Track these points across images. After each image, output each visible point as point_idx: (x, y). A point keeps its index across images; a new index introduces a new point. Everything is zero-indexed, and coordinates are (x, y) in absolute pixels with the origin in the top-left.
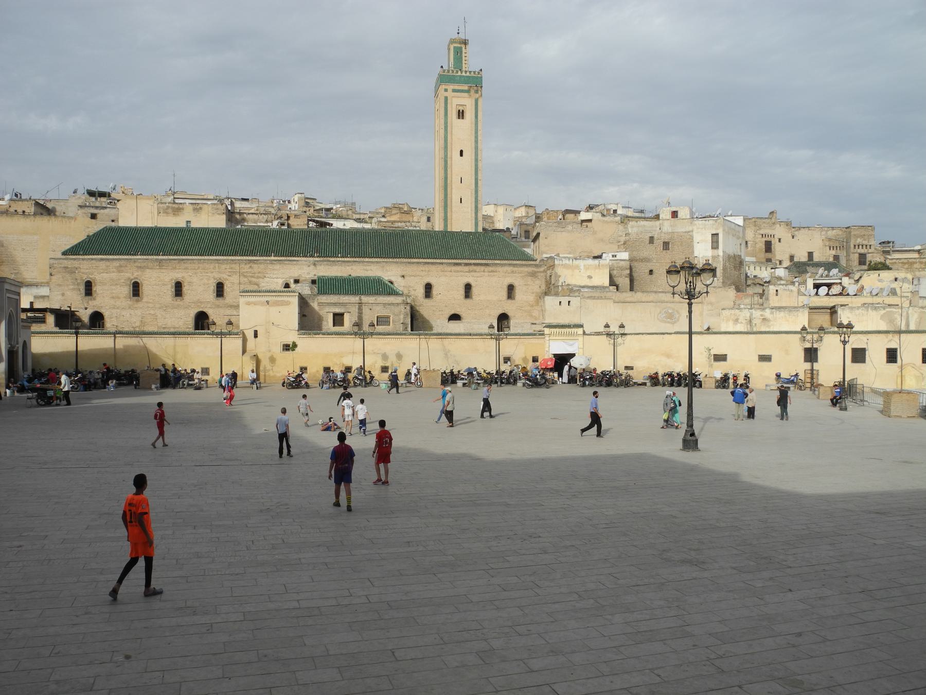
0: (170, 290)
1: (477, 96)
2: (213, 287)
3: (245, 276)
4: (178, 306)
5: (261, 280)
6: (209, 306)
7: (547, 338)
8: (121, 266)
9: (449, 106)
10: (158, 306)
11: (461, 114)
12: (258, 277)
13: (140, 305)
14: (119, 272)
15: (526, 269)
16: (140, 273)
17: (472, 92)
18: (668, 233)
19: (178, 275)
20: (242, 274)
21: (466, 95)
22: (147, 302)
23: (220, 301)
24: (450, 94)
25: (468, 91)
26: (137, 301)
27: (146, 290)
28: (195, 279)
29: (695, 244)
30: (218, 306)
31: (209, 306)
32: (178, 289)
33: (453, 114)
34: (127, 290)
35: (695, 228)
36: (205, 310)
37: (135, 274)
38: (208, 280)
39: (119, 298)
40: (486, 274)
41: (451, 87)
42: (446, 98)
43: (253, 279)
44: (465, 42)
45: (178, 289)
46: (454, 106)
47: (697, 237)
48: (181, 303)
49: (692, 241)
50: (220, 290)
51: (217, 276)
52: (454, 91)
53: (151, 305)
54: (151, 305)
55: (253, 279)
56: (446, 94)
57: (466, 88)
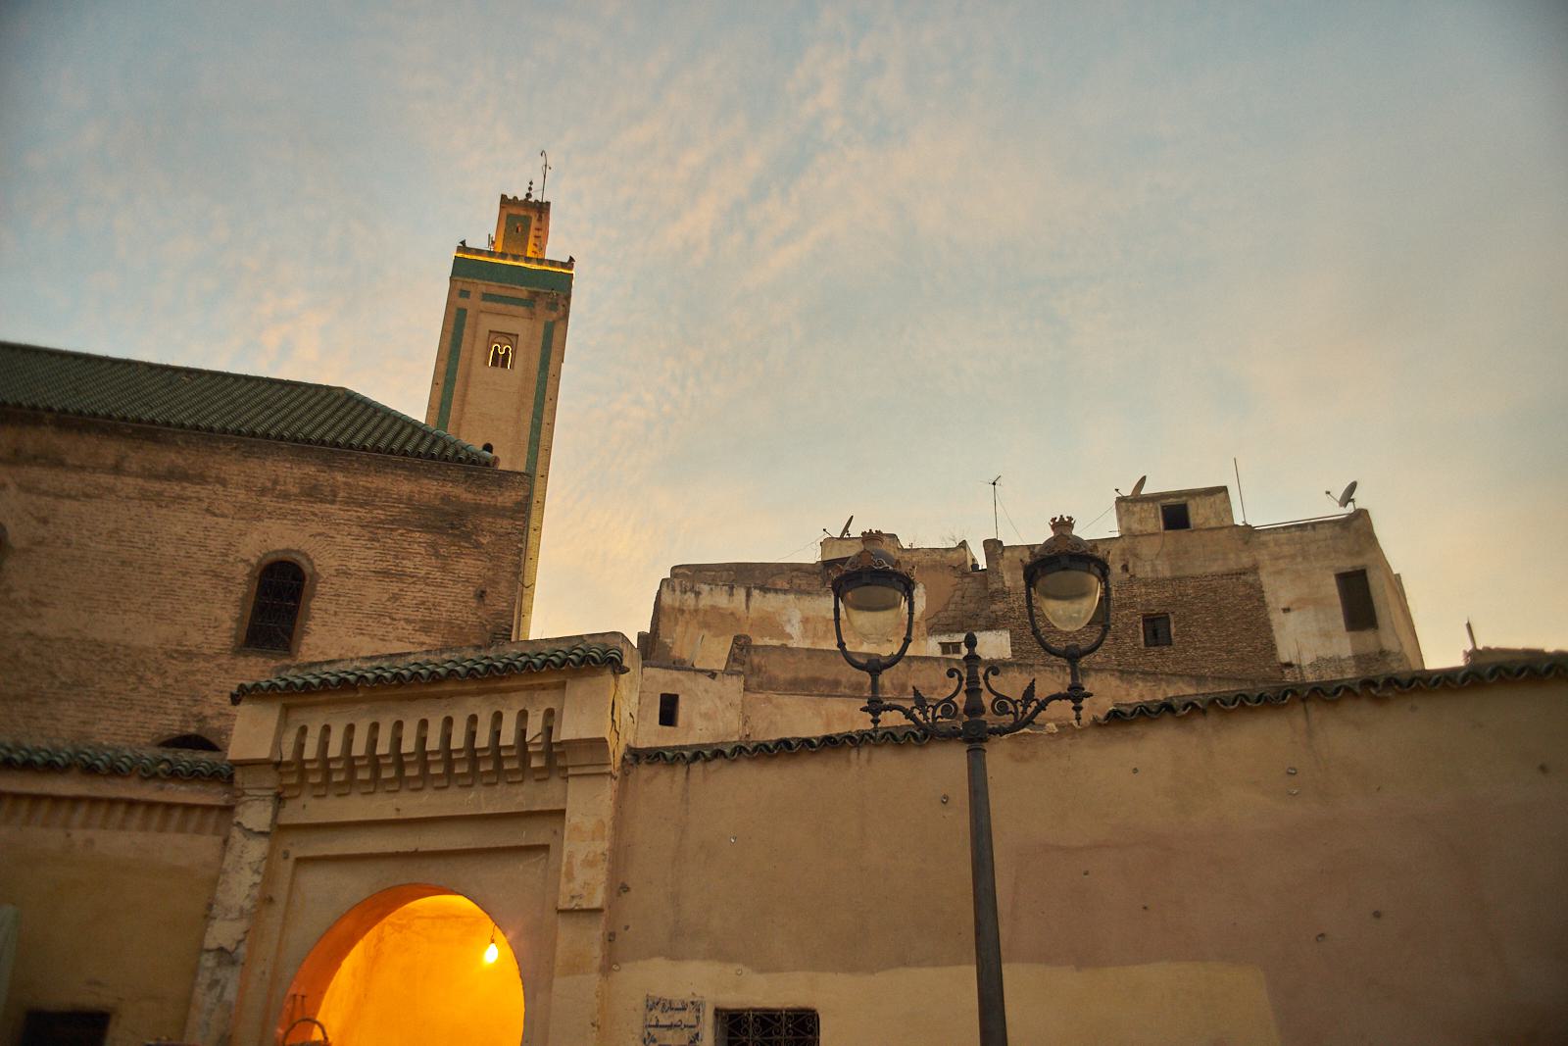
1: (554, 315)
7: (256, 815)
9: (467, 332)
15: (405, 487)
18: (1159, 583)
21: (521, 310)
25: (529, 303)
29: (1276, 618)
35: (1263, 556)
40: (129, 484)
44: (543, 208)
46: (483, 332)
47: (1278, 591)
49: (1262, 604)
52: (486, 297)
56: (462, 302)
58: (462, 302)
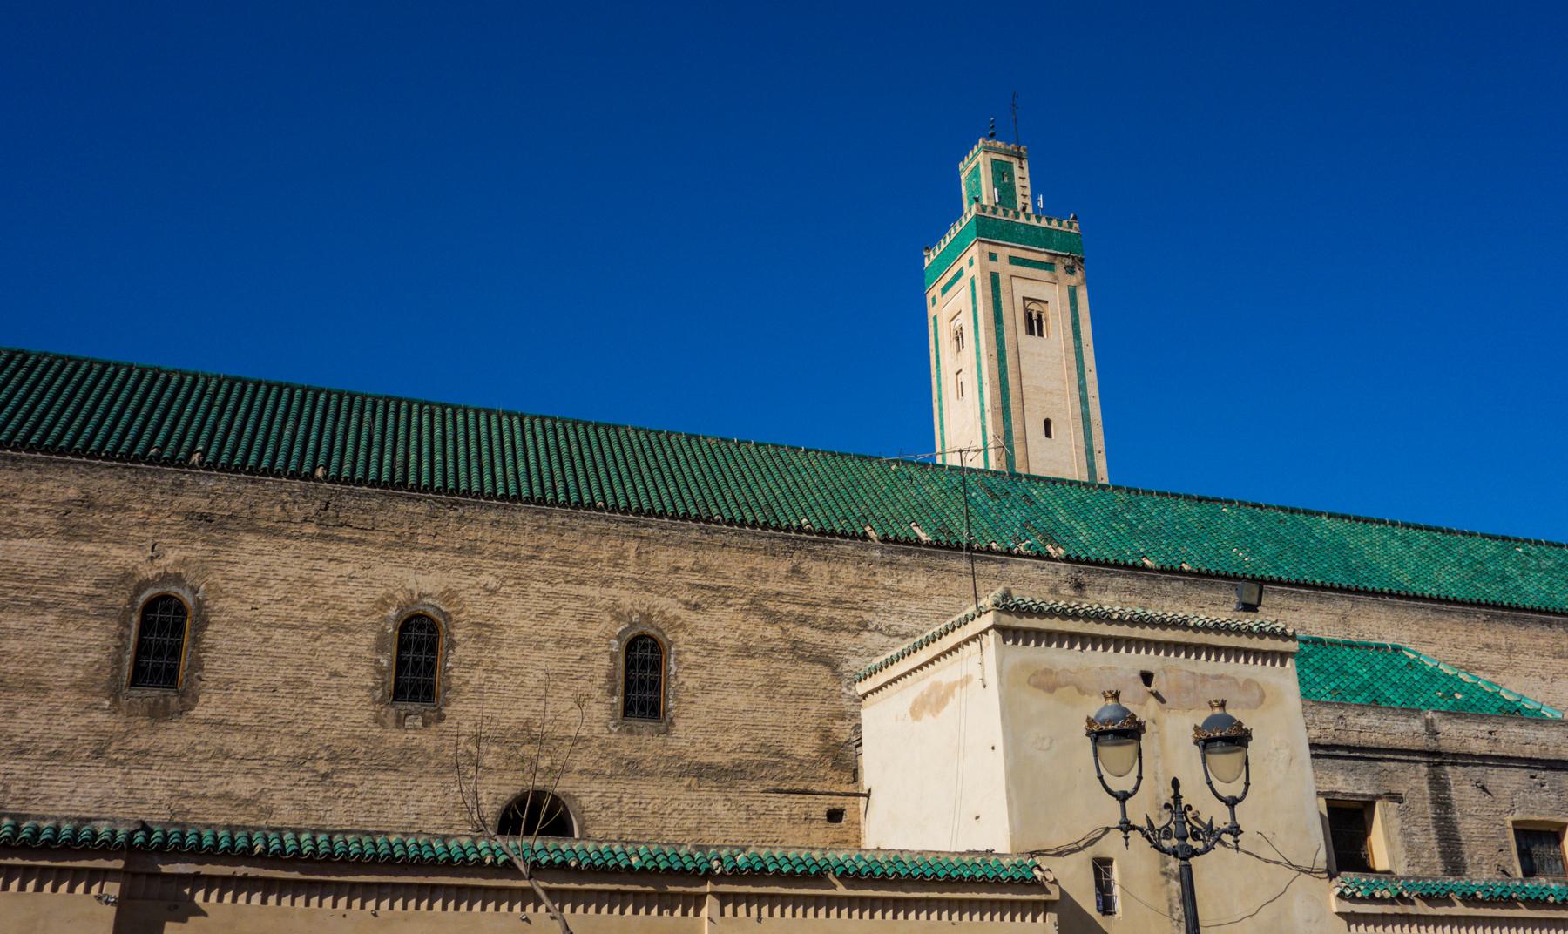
0: (361, 662)
2: (604, 664)
3: (773, 618)
4: (407, 754)
5: (845, 640)
6: (581, 761)
8: (87, 503)
10: (283, 747)
11: (1034, 324)
12: (832, 627)
13: (174, 736)
14: (71, 533)
16: (198, 550)
17: (1060, 270)
19: (420, 579)
20: (757, 606)
22: (219, 724)
23: (645, 743)
24: (1003, 268)
25: (1048, 266)
26: (159, 714)
27: (229, 650)
28: (514, 612)
30: (632, 769)
31: (581, 761)
32: (417, 659)
33: (1014, 321)
34: (93, 644)
36: (563, 786)
37: (171, 557)
38: (585, 619)
39: (37, 687)
41: (1004, 252)
42: (995, 278)
43: (808, 634)
45: (417, 659)
48: (426, 740)
50: (642, 680)
51: (628, 599)
52: (1013, 260)
53: (238, 743)
54: (238, 743)
55: (808, 634)
56: (993, 266)
57: (1044, 258)
58: (993, 266)
